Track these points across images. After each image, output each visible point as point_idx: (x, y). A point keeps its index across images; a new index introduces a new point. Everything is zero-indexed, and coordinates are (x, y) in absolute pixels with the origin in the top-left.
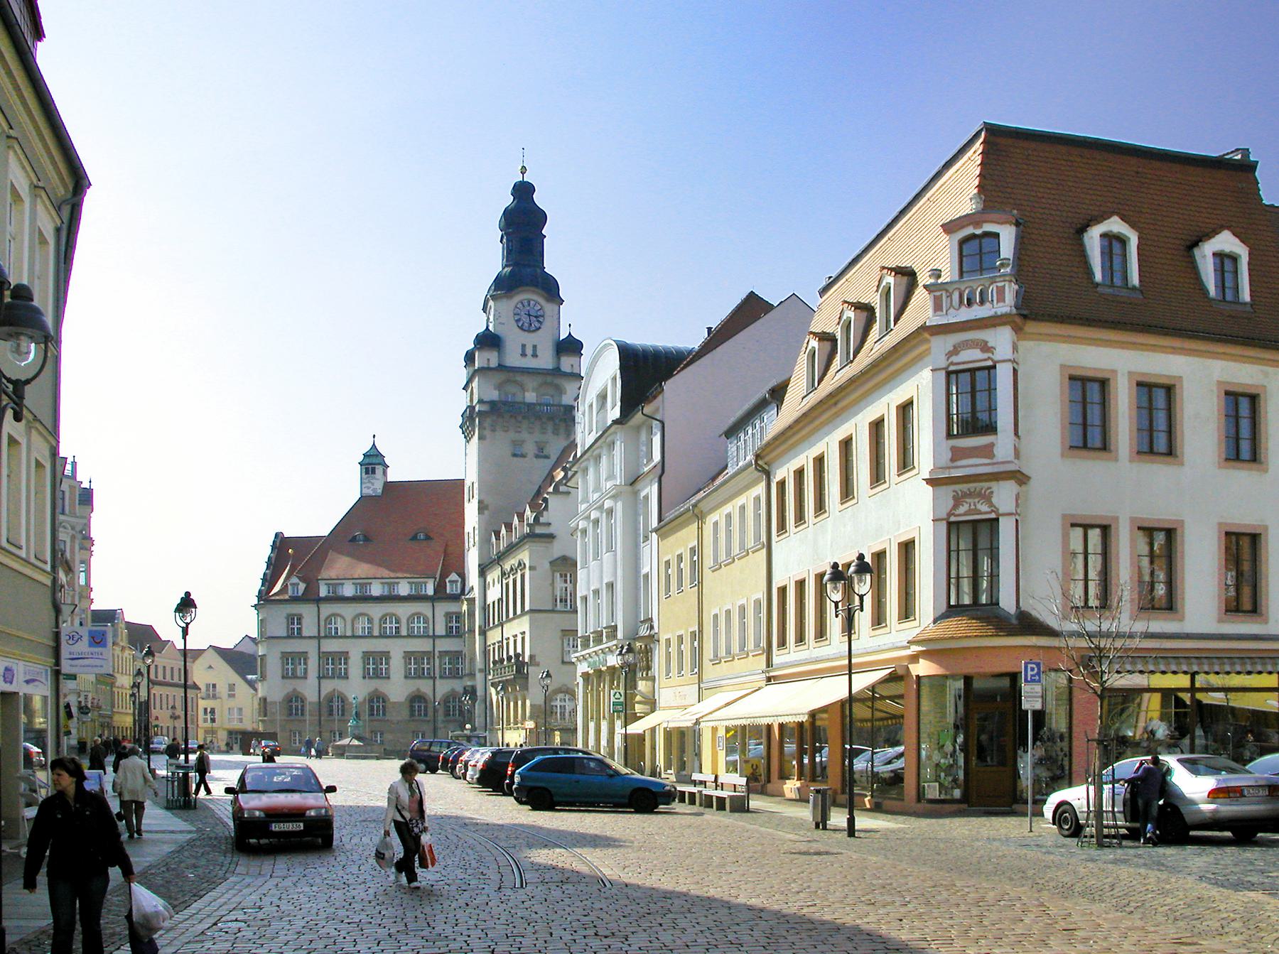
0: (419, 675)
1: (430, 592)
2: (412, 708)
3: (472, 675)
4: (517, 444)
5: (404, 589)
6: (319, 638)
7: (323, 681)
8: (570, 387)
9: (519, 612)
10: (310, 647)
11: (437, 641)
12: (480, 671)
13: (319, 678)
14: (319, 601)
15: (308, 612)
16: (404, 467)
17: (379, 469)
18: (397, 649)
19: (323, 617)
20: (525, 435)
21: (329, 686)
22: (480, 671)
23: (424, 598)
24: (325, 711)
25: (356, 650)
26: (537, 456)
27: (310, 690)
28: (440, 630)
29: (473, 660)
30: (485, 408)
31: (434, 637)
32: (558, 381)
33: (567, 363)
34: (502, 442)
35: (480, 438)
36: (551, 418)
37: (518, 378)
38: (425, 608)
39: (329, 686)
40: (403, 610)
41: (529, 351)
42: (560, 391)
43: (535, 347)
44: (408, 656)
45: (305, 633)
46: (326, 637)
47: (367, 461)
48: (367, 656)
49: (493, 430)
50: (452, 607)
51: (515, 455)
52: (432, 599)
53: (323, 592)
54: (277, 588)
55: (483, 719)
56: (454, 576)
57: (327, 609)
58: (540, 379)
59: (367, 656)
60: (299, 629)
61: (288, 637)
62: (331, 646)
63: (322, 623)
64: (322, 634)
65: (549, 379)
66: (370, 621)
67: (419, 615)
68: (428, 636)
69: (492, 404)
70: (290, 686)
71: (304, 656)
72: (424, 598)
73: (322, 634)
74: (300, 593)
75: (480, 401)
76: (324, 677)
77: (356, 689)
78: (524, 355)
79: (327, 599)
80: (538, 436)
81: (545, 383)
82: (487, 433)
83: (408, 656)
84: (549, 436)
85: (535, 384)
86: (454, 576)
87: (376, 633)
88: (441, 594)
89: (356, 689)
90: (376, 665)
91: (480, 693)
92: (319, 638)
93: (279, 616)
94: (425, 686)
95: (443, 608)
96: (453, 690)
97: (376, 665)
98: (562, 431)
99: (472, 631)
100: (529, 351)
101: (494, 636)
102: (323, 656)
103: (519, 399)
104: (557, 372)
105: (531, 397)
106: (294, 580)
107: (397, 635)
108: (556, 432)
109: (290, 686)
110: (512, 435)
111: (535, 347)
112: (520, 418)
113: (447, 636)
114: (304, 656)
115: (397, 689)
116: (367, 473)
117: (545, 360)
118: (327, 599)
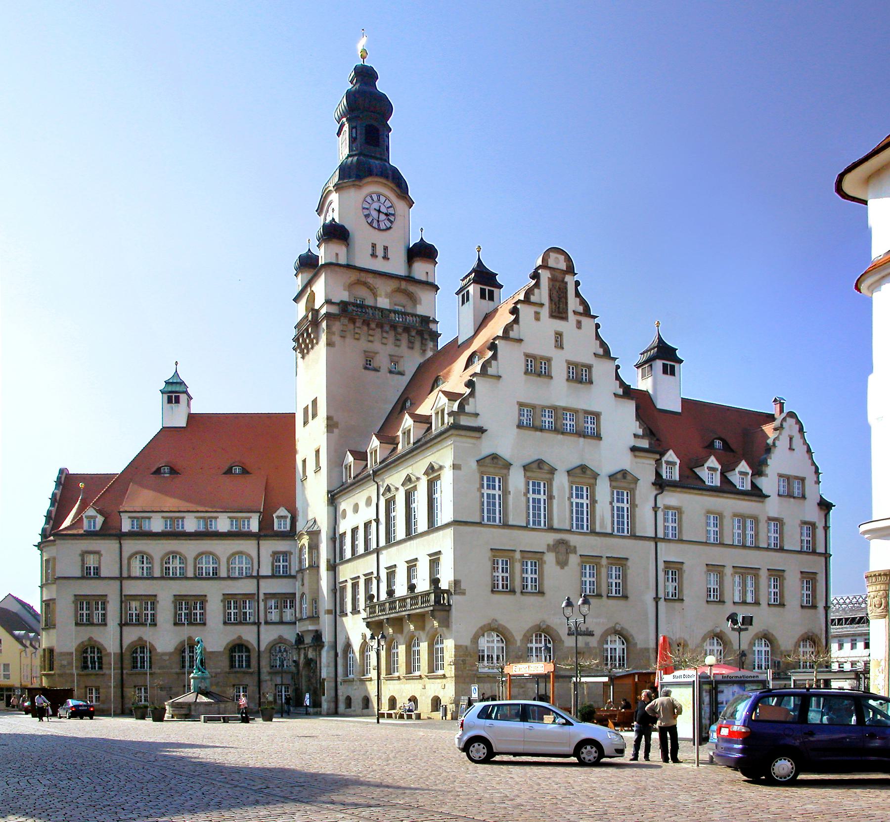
0: (242, 621)
1: (254, 527)
2: (232, 659)
3: (314, 618)
5: (223, 524)
6: (121, 578)
7: (124, 628)
8: (424, 295)
9: (361, 550)
10: (111, 591)
12: (329, 612)
13: (121, 625)
14: (121, 536)
15: (108, 547)
17: (183, 397)
18: (214, 592)
19: (125, 555)
20: (377, 346)
21: (132, 635)
22: (329, 612)
23: (248, 535)
24: (127, 662)
25: (165, 594)
26: (391, 372)
27: (110, 639)
28: (266, 570)
29: (315, 601)
30: (334, 310)
32: (412, 288)
33: (420, 269)
34: (354, 349)
35: (329, 344)
36: (407, 330)
37: (370, 280)
39: (132, 635)
41: (380, 252)
42: (413, 299)
43: (386, 249)
44: (228, 599)
45: (103, 574)
46: (130, 578)
47: (170, 388)
48: (179, 599)
49: (343, 337)
51: (366, 368)
53: (126, 526)
54: (67, 523)
55: (332, 669)
57: (130, 546)
58: (392, 285)
59: (179, 599)
60: (97, 569)
61: (83, 578)
62: (132, 588)
63: (125, 562)
64: (125, 574)
65: (404, 285)
66: (183, 560)
68: (252, 577)
69: (343, 305)
70: (86, 634)
71: (102, 600)
73: (125, 574)
74: (98, 528)
75: (328, 302)
76: (126, 624)
77: (164, 638)
79: (132, 535)
80: (390, 348)
81: (399, 290)
82: (336, 339)
83: (228, 599)
84: (404, 349)
85: (389, 290)
86: (282, 511)
87: (190, 574)
89: (164, 638)
90: (190, 611)
91: (327, 638)
93: (69, 558)
95: (269, 547)
97: (190, 611)
98: (417, 345)
99: (315, 567)
100: (380, 252)
101: (346, 572)
102: (125, 600)
103: (369, 302)
104: (409, 279)
105: (383, 302)
106: (91, 512)
107: (215, 576)
109: (86, 634)
110: (363, 344)
111: (386, 249)
112: (373, 325)
113: (273, 576)
114: (102, 600)
115: (215, 637)
116: (170, 401)
117: (397, 265)
118: (132, 535)
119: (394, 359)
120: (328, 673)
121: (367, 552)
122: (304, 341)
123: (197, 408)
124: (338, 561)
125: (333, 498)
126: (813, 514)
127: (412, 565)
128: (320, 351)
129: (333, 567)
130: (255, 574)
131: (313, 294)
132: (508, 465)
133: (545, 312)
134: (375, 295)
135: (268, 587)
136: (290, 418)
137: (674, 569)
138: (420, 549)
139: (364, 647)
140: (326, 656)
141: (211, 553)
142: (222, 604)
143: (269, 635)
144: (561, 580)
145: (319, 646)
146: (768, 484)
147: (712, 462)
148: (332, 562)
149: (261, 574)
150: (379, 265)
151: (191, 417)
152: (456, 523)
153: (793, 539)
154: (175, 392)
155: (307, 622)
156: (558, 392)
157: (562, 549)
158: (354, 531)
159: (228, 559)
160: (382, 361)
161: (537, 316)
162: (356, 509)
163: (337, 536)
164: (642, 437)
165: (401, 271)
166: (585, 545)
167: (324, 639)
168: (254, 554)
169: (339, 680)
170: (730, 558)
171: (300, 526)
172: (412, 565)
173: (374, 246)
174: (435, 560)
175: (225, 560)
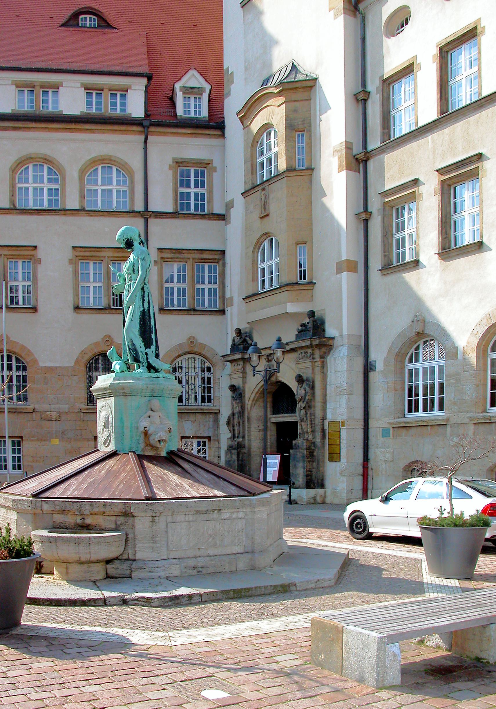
3: (302, 282)
5: (71, 98)
11: (154, 224)
28: (162, 200)
31: (146, 215)
38: (124, 146)
40: (71, 149)
50: (195, 147)
52: (147, 125)
56: (193, 79)
67: (107, 161)
68: (133, 213)
72: (124, 122)
86: (193, 79)
88: (160, 117)
91: (342, 325)
96: (192, 341)
99: (303, 171)
120: (350, 408)
124: (374, 144)
129: (359, 161)
130: (139, 206)
135: (169, 234)
140: (341, 369)
141: (47, 160)
142: (71, 269)
145: (320, 346)
148: (358, 149)
149: (151, 208)
155: (284, 295)
159: (82, 172)
163: (373, 86)
167: (330, 331)
168: (137, 165)
169: (377, 424)
175: (76, 175)
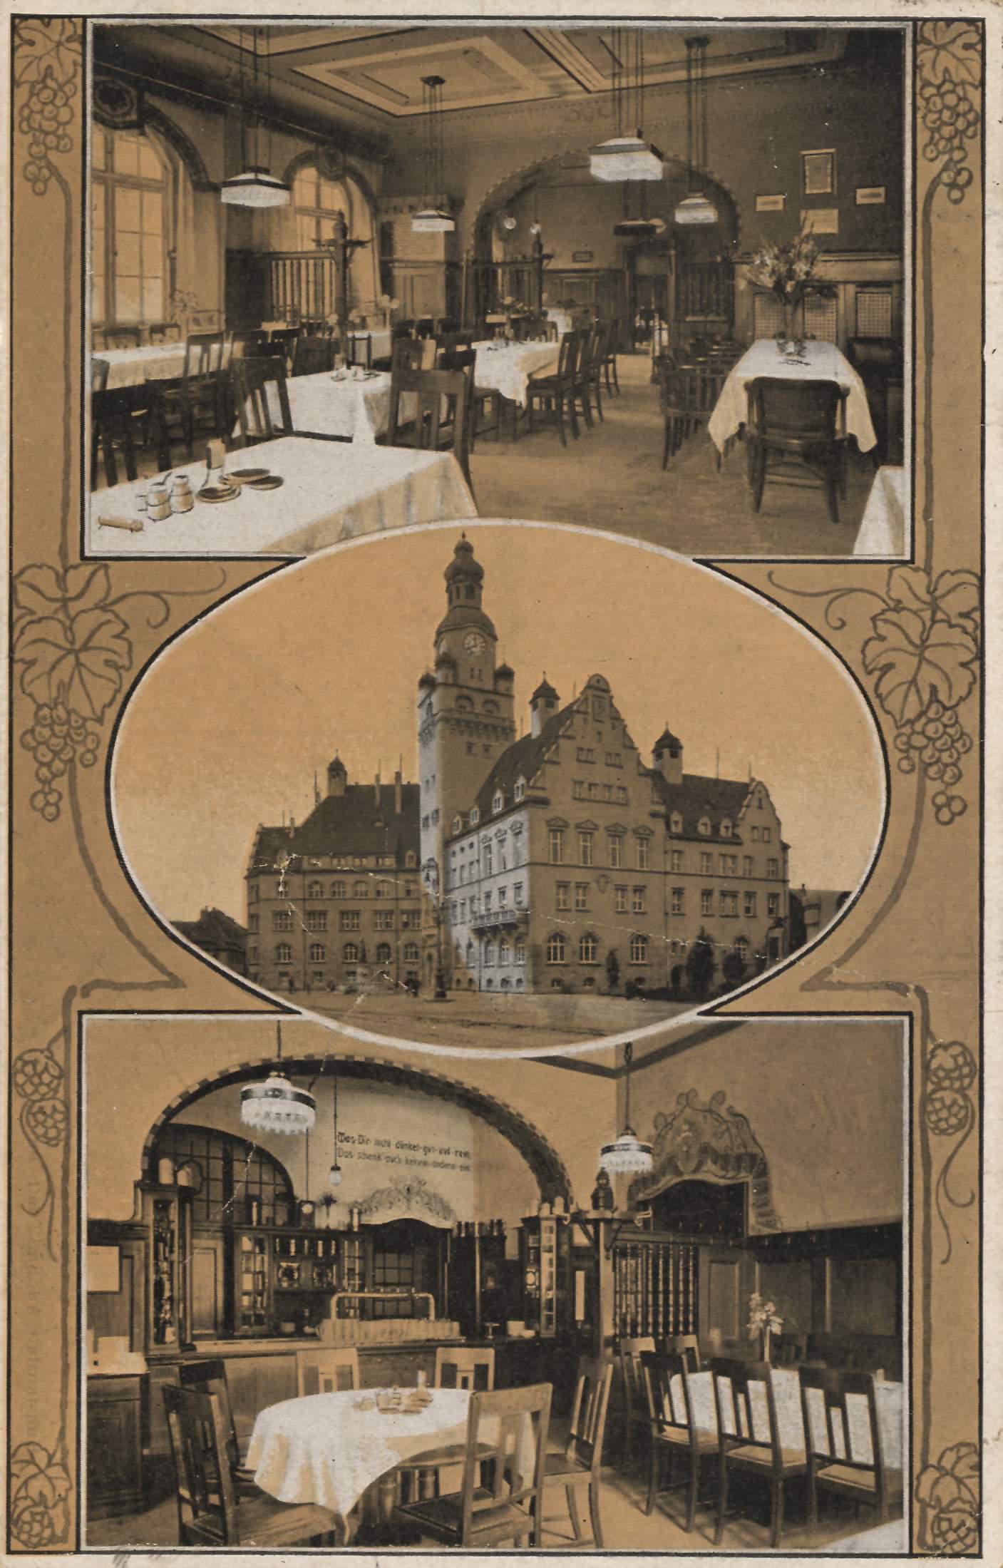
4: (470, 747)
6: (304, 900)
16: (365, 771)
20: (474, 739)
31: (397, 899)
32: (497, 698)
33: (502, 685)
41: (476, 673)
56: (410, 853)
58: (482, 697)
62: (310, 906)
65: (492, 697)
78: (472, 677)
80: (485, 741)
92: (304, 900)
94: (389, 938)
100: (476, 673)
104: (495, 692)
108: (497, 739)
110: (466, 737)
119: (487, 748)
121: (471, 883)
122: (425, 736)
123: (351, 781)
125: (447, 843)
126: (777, 854)
127: (502, 892)
128: (435, 744)
131: (430, 704)
132: (566, 825)
133: (590, 718)
134: (473, 705)
136: (417, 787)
137: (678, 892)
138: (508, 881)
139: (470, 946)
143: (405, 937)
144: (603, 900)
146: (744, 832)
147: (705, 820)
150: (472, 684)
151: (349, 789)
152: (531, 864)
153: (760, 870)
154: (336, 769)
156: (600, 773)
157: (602, 880)
158: (462, 867)
160: (478, 749)
161: (585, 721)
162: (462, 849)
164: (657, 803)
165: (489, 685)
166: (617, 878)
170: (716, 885)
171: (424, 861)
172: (502, 892)
173: (472, 670)
174: (518, 887)
